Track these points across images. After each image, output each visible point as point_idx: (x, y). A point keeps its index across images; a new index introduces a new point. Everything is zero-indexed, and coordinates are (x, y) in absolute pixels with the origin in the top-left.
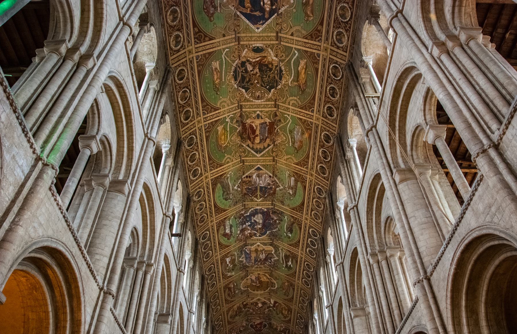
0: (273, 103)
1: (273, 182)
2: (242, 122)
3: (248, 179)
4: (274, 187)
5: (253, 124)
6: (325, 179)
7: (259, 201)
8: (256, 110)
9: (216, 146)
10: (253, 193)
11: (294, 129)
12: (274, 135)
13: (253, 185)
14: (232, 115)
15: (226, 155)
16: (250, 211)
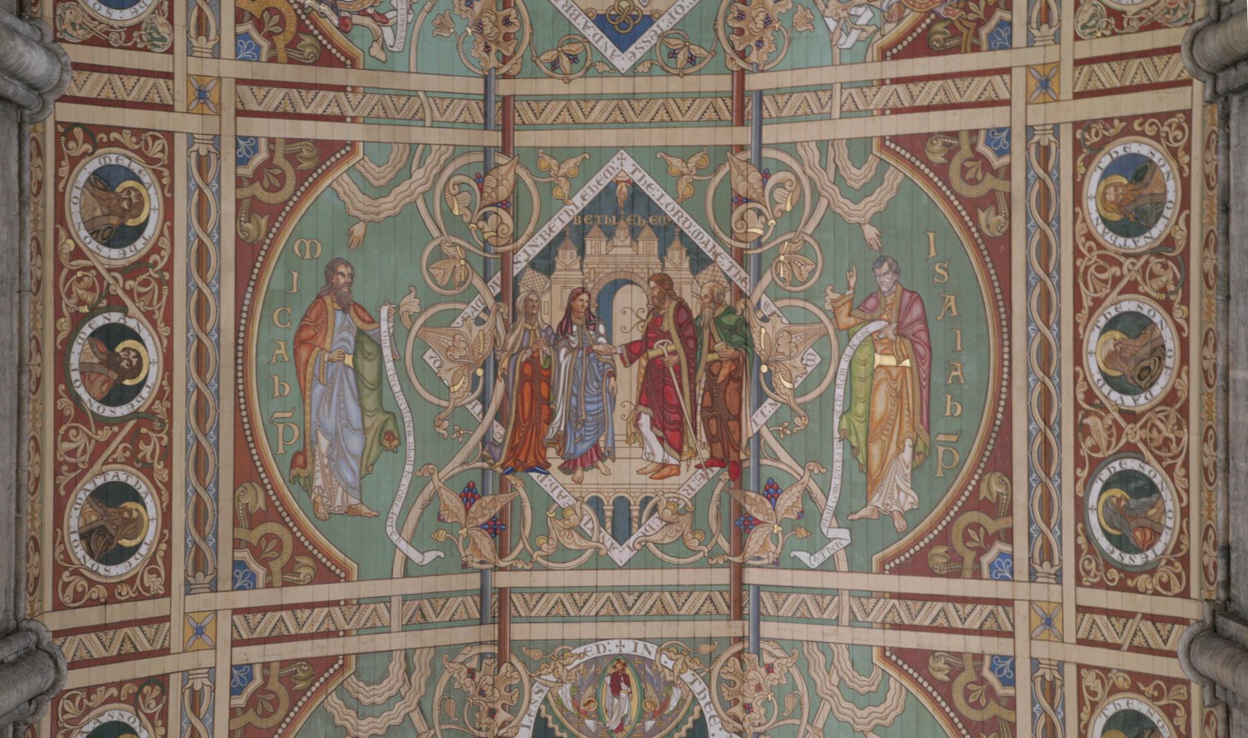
0: (519, 632)
2: (737, 472)
5: (659, 453)
6: (91, 132)
8: (638, 578)
9: (938, 350)
11: (367, 468)
12: (513, 356)
14: (803, 556)
15: (870, 232)
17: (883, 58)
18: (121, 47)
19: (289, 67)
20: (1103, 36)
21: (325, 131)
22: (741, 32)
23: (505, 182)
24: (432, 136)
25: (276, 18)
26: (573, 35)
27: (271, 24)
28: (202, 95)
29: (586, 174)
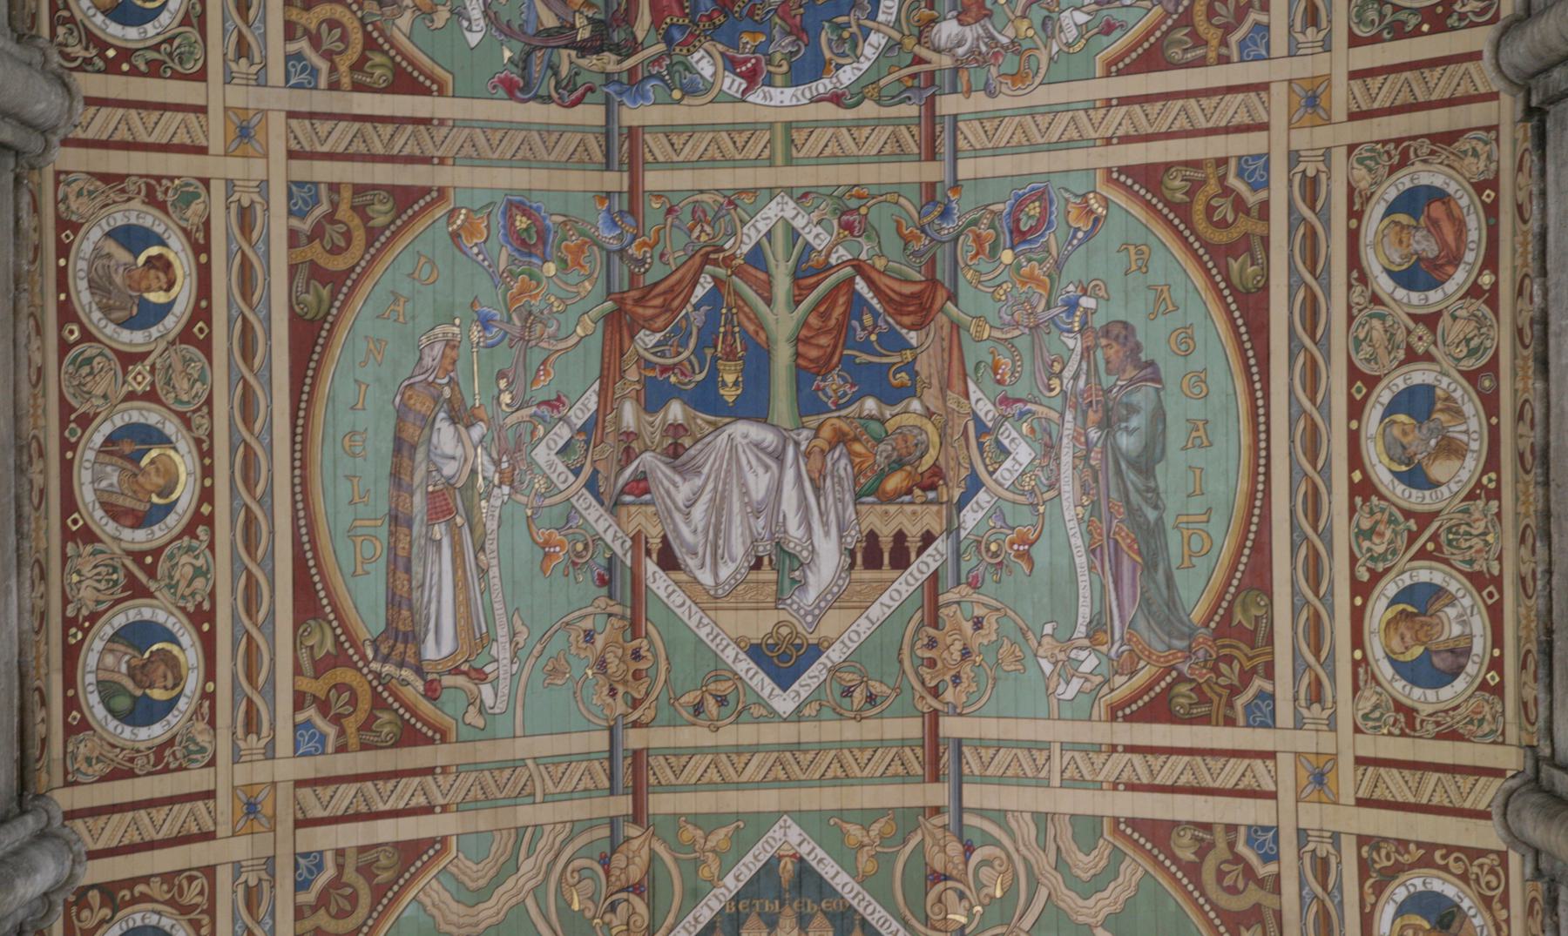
1: (640, 485)
3: (885, 522)
4: (629, 414)
7: (772, 211)
10: (843, 328)
13: (840, 438)
16: (870, 50)
17: (1114, 718)
18: (150, 774)
19: (362, 755)
20: (1390, 734)
21: (409, 829)
22: (932, 663)
23: (637, 860)
24: (543, 814)
25: (346, 696)
26: (720, 672)
27: (340, 703)
28: (252, 808)
29: (740, 845)
